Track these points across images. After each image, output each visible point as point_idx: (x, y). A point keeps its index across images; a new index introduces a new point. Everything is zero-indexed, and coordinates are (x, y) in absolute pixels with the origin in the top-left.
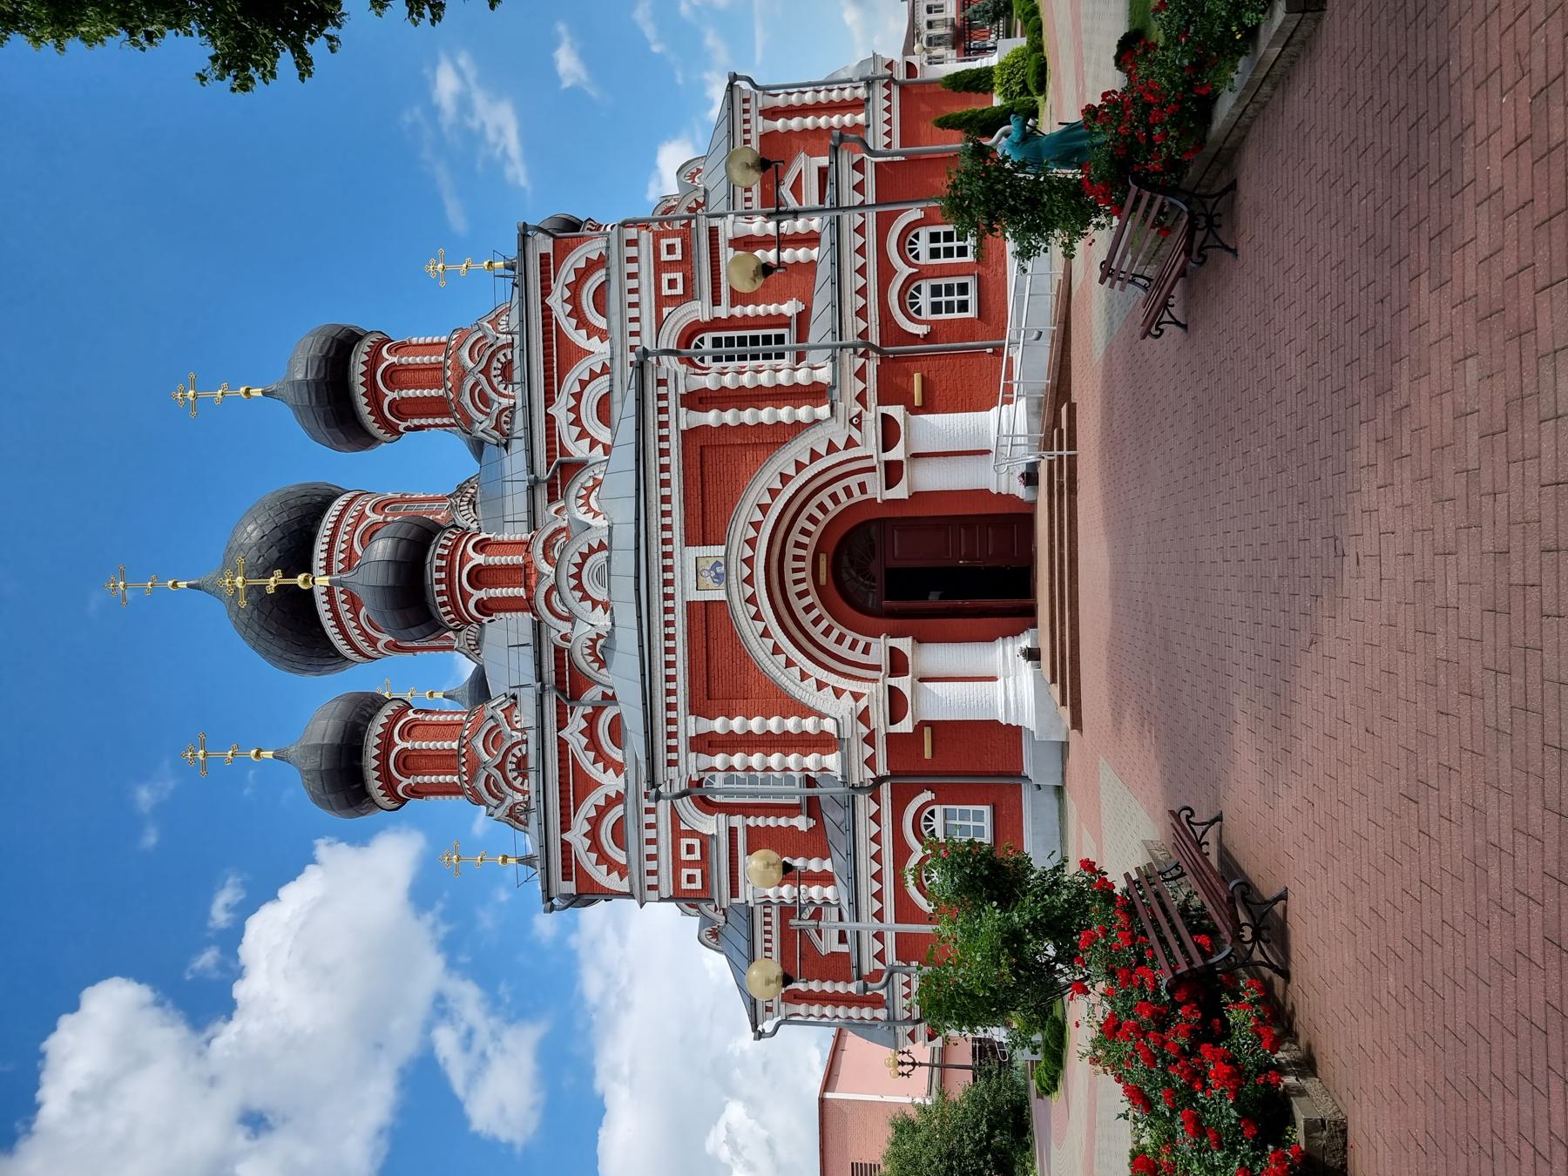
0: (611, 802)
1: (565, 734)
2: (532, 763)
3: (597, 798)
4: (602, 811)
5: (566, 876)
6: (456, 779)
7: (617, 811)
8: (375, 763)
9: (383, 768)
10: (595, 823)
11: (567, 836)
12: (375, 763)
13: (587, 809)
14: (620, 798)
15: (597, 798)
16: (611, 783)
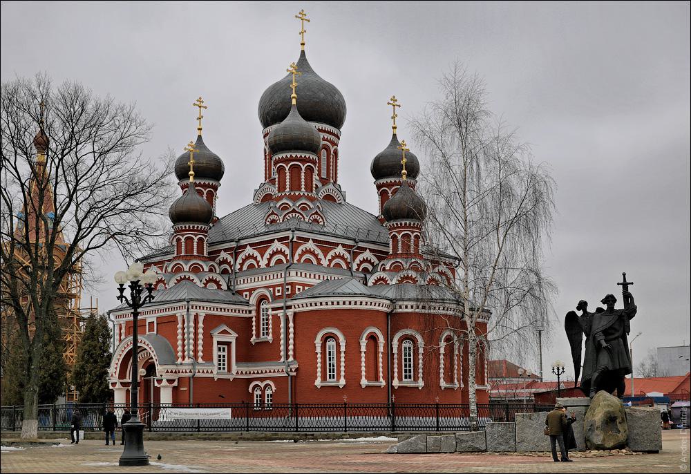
0: (319, 260)
1: (340, 246)
2: (316, 228)
3: (321, 256)
4: (316, 256)
5: (298, 238)
6: (288, 190)
7: (315, 262)
8: (294, 156)
9: (292, 159)
10: (313, 253)
11: (311, 241)
12: (294, 156)
13: (318, 251)
14: (319, 263)
15: (321, 256)
16: (325, 262)
